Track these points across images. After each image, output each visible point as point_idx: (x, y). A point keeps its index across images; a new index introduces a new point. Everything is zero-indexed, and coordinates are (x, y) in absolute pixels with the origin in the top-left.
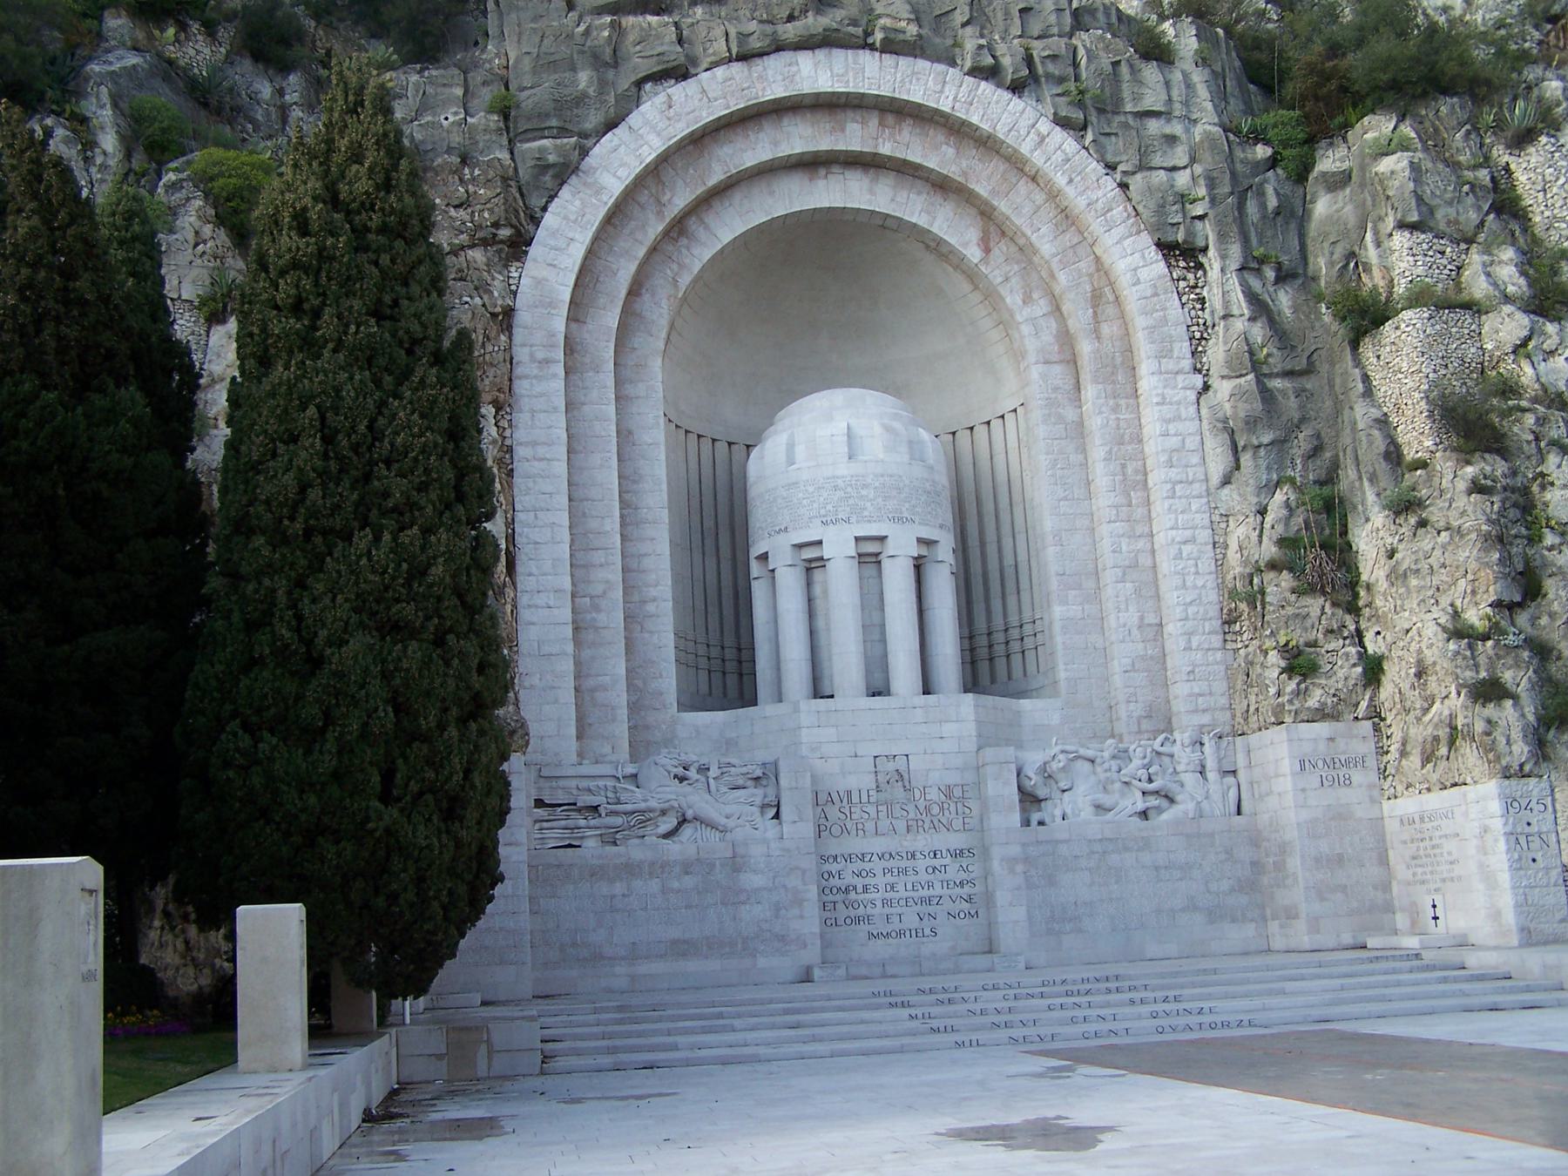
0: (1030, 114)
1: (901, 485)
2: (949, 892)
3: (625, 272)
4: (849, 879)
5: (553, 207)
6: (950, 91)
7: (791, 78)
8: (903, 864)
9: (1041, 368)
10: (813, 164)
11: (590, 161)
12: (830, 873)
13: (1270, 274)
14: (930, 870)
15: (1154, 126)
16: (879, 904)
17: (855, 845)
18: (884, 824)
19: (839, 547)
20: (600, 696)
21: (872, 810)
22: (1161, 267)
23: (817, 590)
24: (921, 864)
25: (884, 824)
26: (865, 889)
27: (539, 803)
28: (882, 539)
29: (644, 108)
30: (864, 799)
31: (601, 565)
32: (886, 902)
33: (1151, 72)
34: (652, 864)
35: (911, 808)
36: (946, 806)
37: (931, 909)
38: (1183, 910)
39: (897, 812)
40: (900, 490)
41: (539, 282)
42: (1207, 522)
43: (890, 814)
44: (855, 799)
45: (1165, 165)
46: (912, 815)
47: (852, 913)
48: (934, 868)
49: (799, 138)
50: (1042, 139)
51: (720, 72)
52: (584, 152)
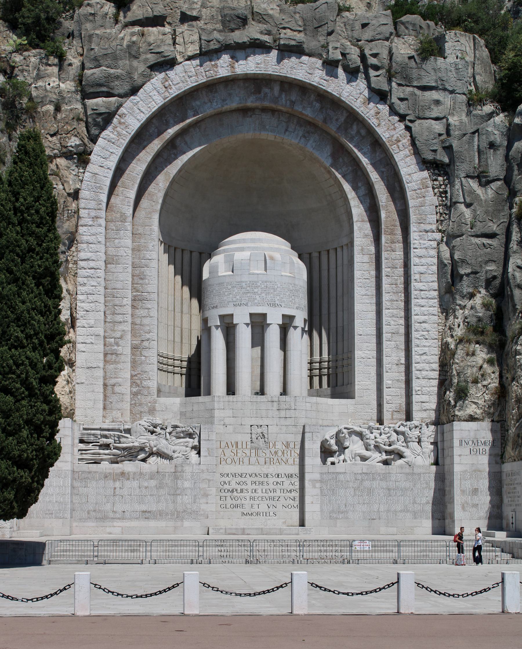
1: (276, 287)
2: (284, 495)
4: (234, 486)
8: (262, 479)
11: (122, 110)
12: (225, 483)
14: (275, 483)
16: (248, 498)
18: (253, 460)
24: (271, 480)
25: (253, 460)
26: (242, 491)
27: (82, 441)
28: (264, 316)
30: (244, 446)
31: (120, 322)
32: (253, 498)
34: (135, 473)
36: (285, 452)
37: (274, 503)
38: (401, 511)
43: (257, 455)
44: (240, 446)
45: (432, 116)
46: (268, 455)
47: (234, 502)
48: (277, 483)
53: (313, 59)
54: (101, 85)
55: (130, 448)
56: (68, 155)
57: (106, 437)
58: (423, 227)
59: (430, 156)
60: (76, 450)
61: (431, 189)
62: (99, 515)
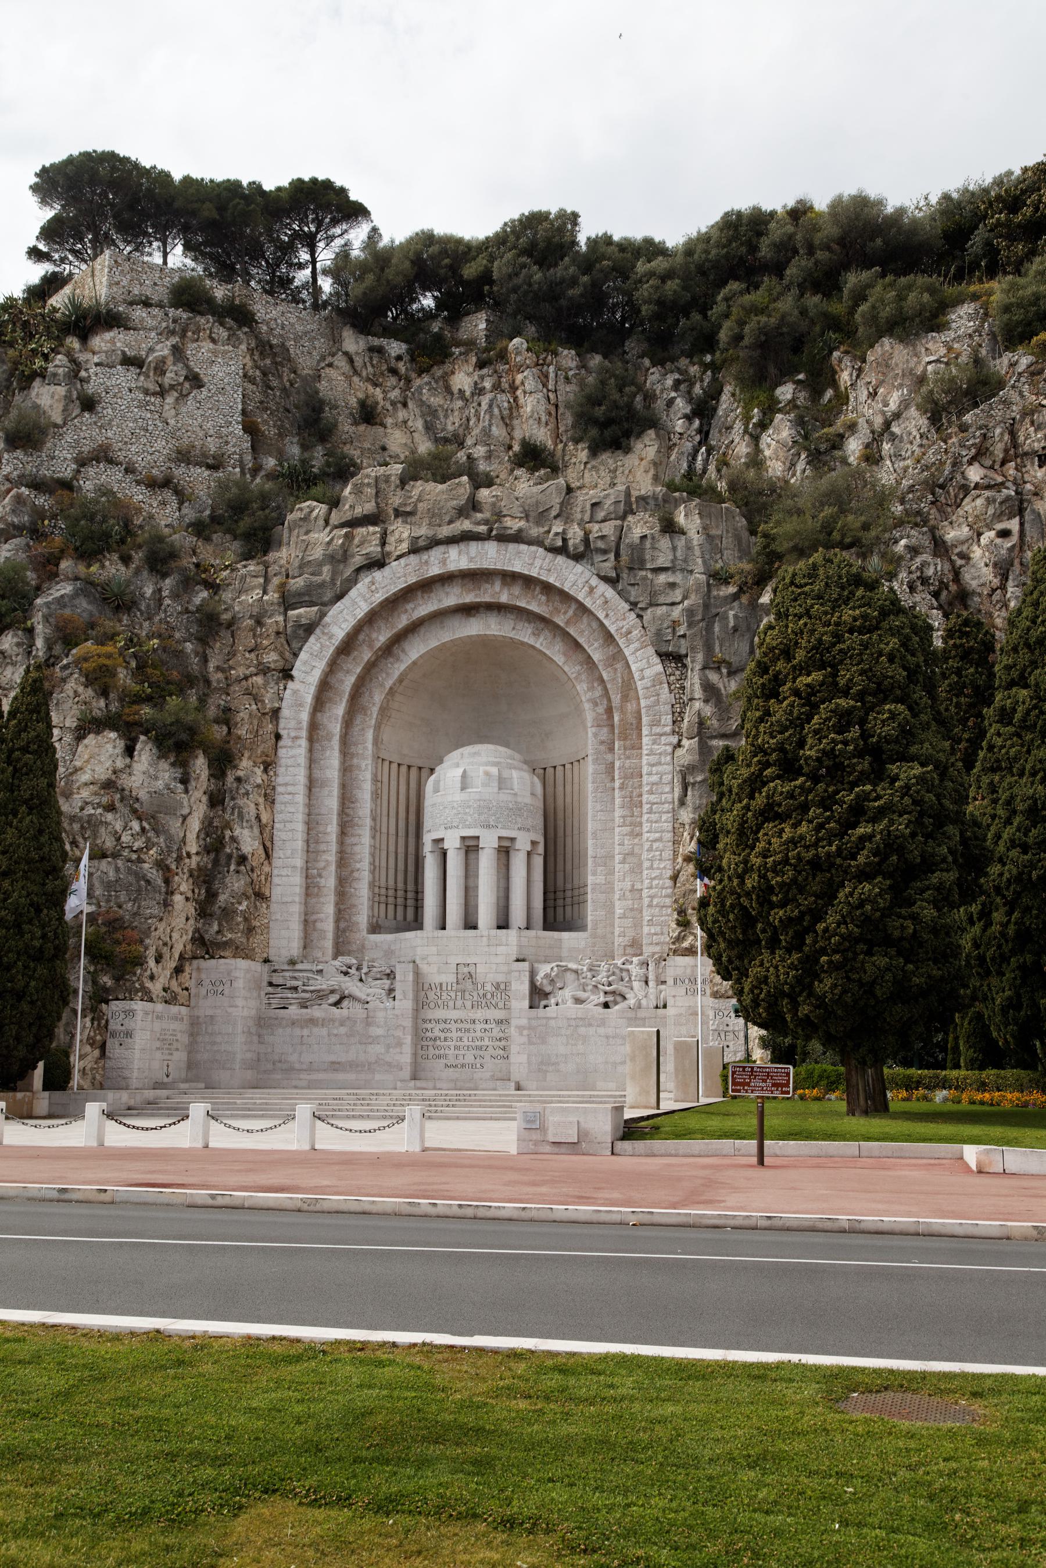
0: (588, 574)
3: (348, 682)
4: (437, 1033)
5: (305, 648)
6: (538, 563)
7: (444, 562)
8: (468, 1026)
9: (594, 730)
10: (468, 610)
11: (327, 619)
13: (724, 671)
15: (662, 578)
17: (440, 1014)
18: (459, 1003)
19: (452, 843)
20: (319, 925)
21: (453, 994)
22: (659, 668)
23: (472, 862)
24: (479, 1026)
26: (446, 1039)
27: (271, 984)
28: (478, 838)
29: (359, 586)
32: (456, 1048)
33: (665, 543)
35: (475, 994)
39: (467, 996)
40: (489, 809)
41: (295, 692)
42: (670, 828)
43: (463, 998)
47: (437, 1052)
49: (452, 597)
50: (592, 589)
51: (402, 561)
52: (323, 615)
53: (533, 548)
54: (304, 594)
55: (319, 991)
56: (264, 670)
57: (295, 978)
58: (657, 730)
59: (664, 649)
60: (263, 993)
61: (666, 685)
62: (285, 1066)
